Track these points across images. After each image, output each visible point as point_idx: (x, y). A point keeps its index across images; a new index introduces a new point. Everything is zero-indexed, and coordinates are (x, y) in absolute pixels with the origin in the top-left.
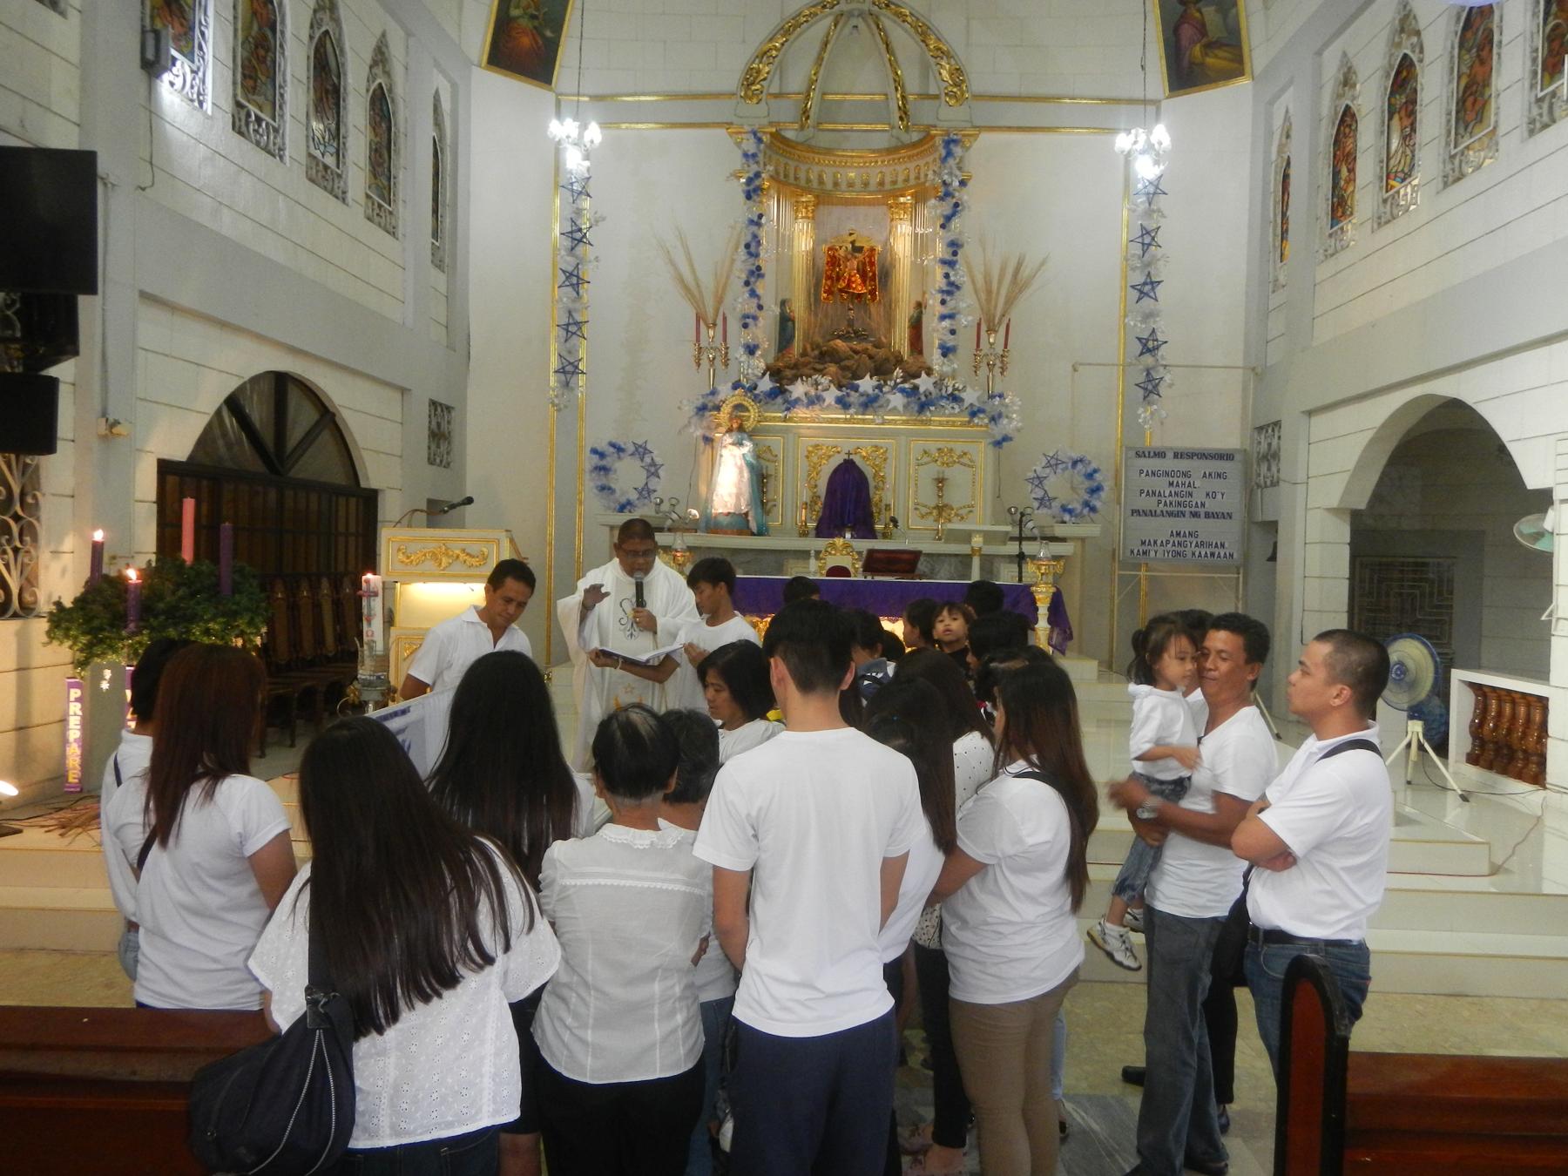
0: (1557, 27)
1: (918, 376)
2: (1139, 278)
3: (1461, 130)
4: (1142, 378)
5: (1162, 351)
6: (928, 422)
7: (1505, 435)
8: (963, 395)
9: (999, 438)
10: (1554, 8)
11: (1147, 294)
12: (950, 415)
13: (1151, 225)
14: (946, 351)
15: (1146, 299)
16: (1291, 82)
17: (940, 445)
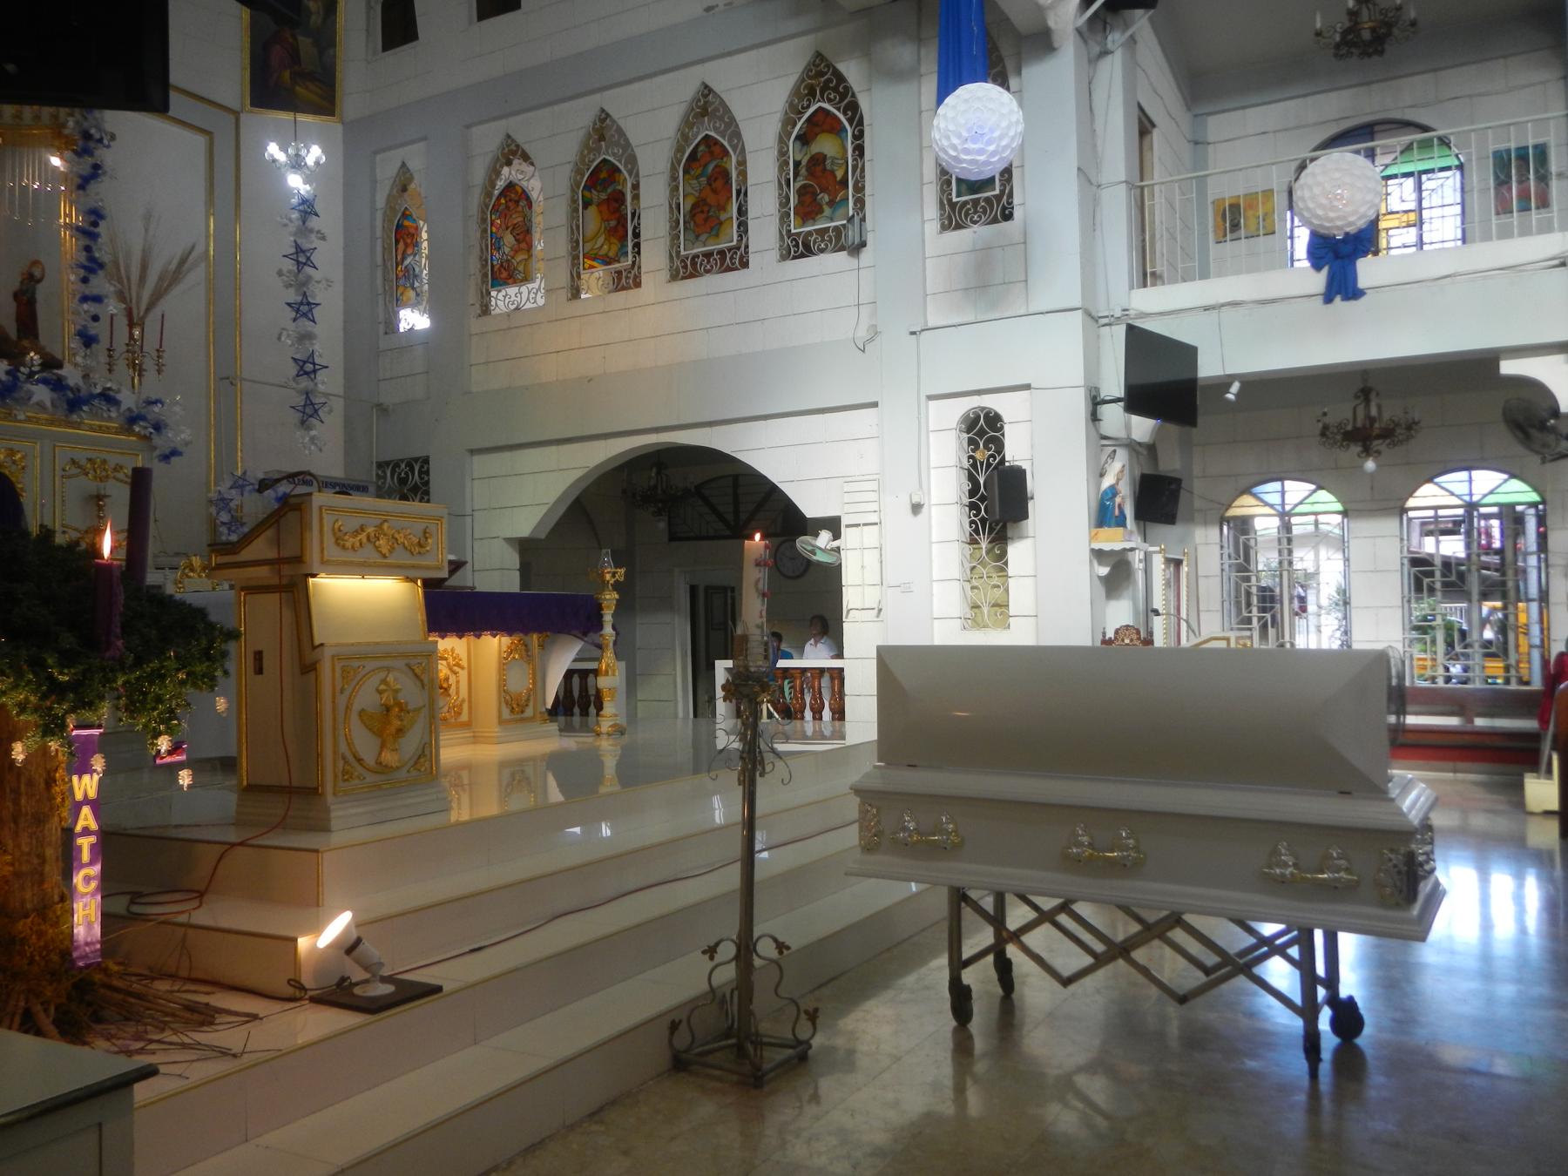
0: (804, 187)
1: (60, 366)
2: (292, 296)
3: (691, 236)
4: (300, 400)
5: (321, 375)
6: (78, 426)
7: (774, 478)
8: (119, 397)
9: (167, 452)
10: (803, 171)
11: (305, 315)
12: (110, 419)
13: (306, 246)
14: (88, 340)
15: (304, 322)
16: (425, 139)
17: (90, 455)
